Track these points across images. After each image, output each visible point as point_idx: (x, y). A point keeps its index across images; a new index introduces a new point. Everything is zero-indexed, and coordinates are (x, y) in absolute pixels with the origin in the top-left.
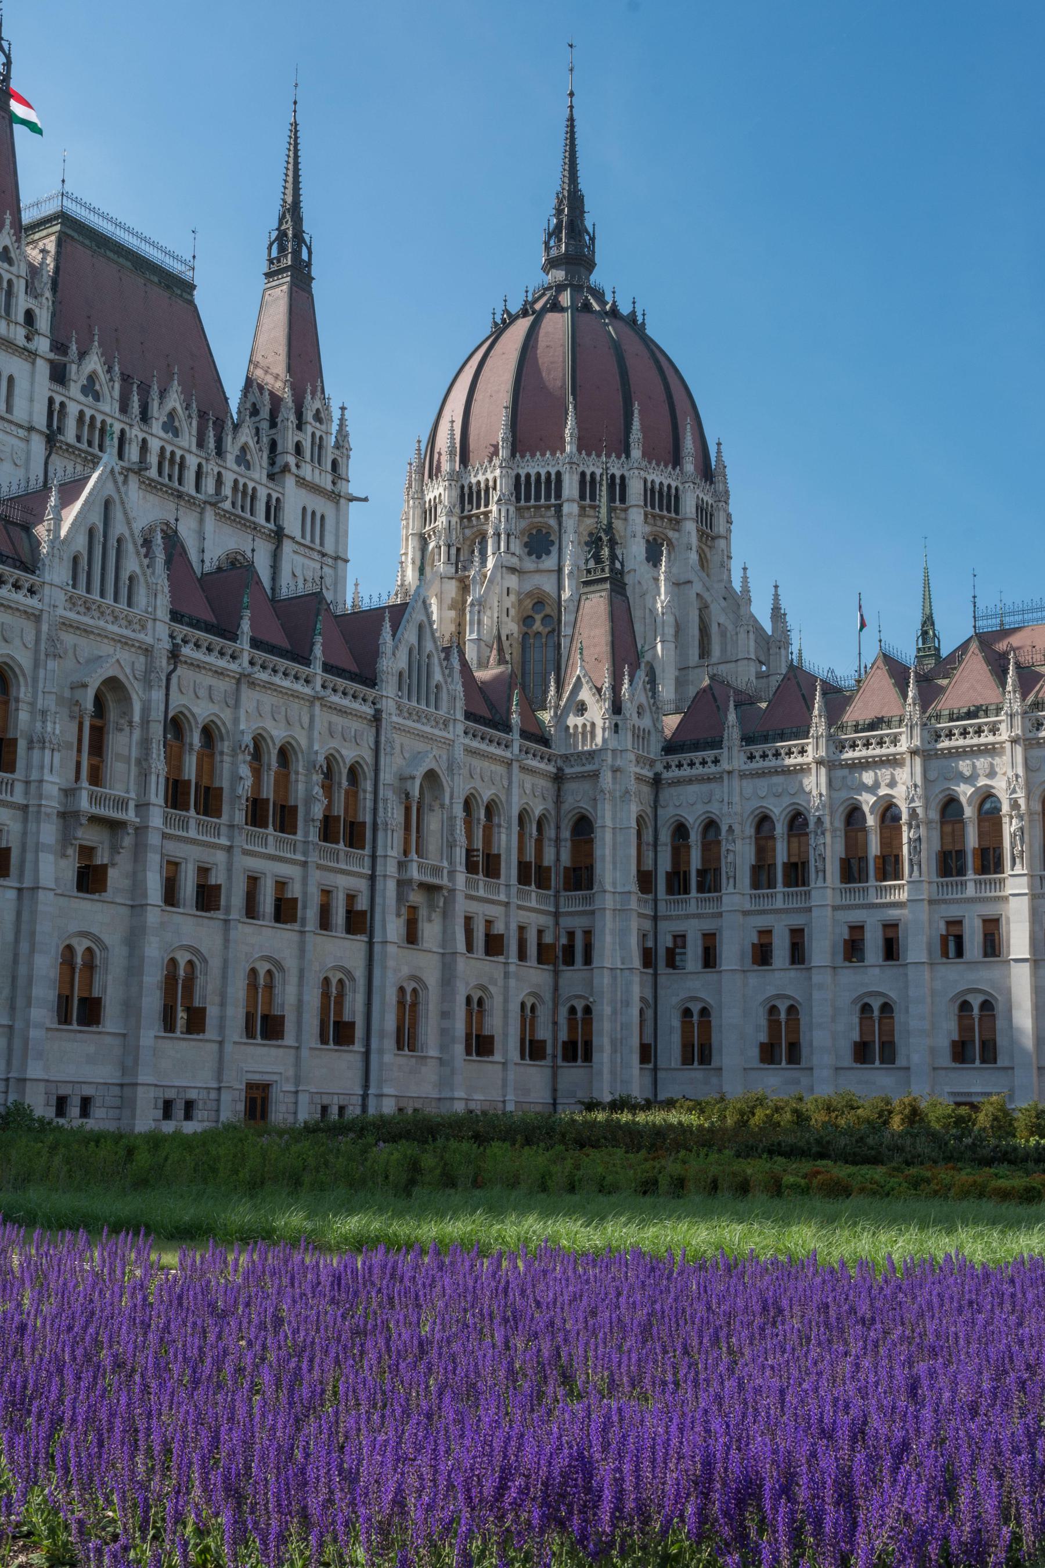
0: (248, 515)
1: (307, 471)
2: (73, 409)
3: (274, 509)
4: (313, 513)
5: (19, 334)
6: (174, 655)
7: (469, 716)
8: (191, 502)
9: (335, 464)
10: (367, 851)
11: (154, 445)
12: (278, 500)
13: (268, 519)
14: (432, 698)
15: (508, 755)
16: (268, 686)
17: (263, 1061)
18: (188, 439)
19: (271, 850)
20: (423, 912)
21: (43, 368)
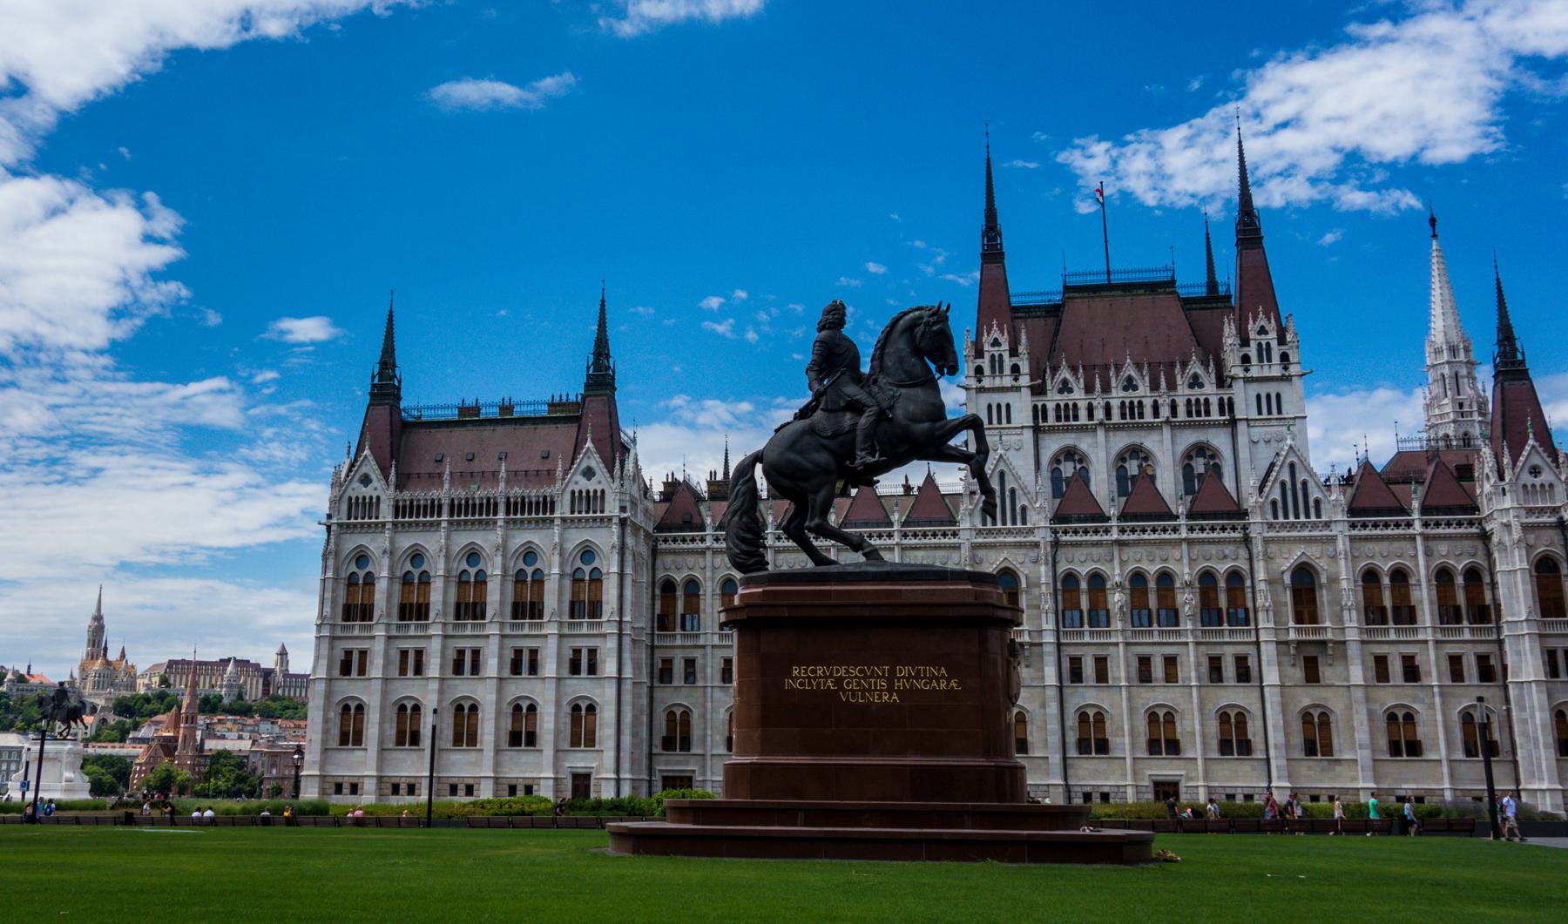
0: (1203, 418)
1: (1255, 372)
2: (1051, 406)
3: (1227, 406)
4: (1268, 396)
5: (1007, 381)
6: (1056, 544)
7: (1352, 511)
8: (1151, 427)
9: (1284, 357)
10: (1252, 626)
11: (1115, 404)
12: (1230, 399)
13: (1222, 413)
14: (1312, 511)
15: (1411, 531)
16: (1137, 543)
17: (1166, 769)
18: (1143, 389)
19: (1156, 639)
20: (1320, 660)
21: (1026, 393)
